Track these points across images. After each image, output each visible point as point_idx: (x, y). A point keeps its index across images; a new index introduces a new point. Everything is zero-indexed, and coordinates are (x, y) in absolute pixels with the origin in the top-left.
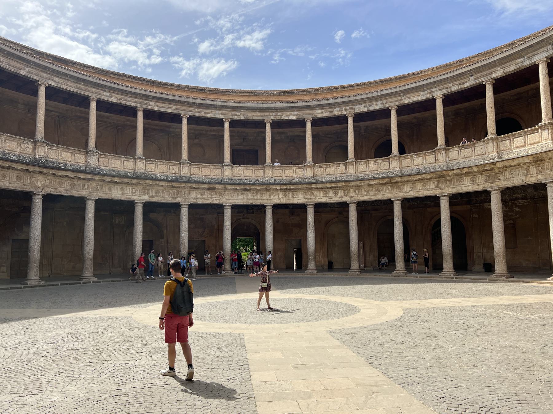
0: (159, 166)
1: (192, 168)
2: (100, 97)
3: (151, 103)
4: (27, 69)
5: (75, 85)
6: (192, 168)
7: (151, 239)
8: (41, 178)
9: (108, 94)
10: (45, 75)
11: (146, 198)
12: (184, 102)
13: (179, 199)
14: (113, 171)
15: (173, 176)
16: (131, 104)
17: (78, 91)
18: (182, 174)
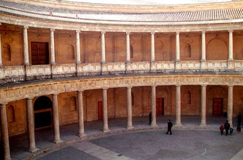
0: (216, 64)
1: (236, 64)
2: (181, 31)
3: (210, 27)
4: (145, 29)
5: (167, 29)
6: (236, 64)
7: (222, 97)
8: (154, 79)
9: (185, 28)
10: (153, 29)
11: (207, 83)
12: (229, 23)
13: (227, 84)
14: (189, 70)
15: (223, 69)
16: (198, 30)
17: (169, 31)
18: (229, 68)
